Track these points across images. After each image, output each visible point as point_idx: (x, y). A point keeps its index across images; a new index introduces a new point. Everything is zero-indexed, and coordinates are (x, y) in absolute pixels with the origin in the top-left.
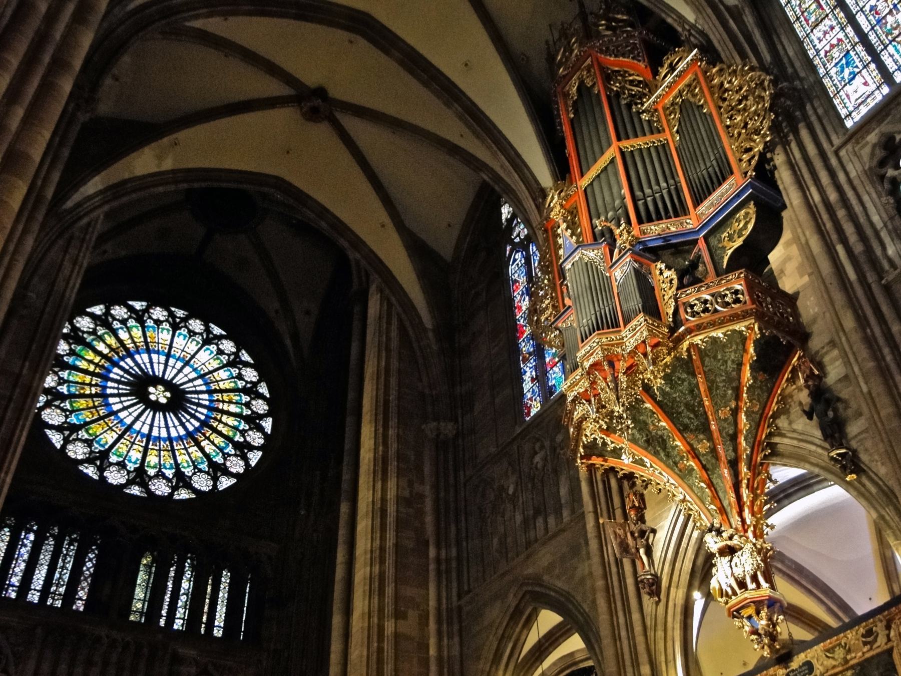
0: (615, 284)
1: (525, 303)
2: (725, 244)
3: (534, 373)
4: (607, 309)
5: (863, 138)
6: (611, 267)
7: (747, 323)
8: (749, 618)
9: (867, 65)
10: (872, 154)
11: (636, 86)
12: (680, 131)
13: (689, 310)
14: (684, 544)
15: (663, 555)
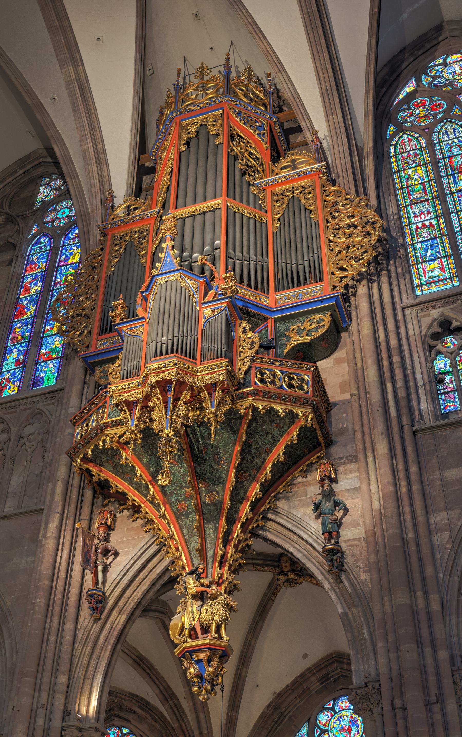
0: (202, 321)
1: (36, 288)
2: (292, 335)
3: (21, 357)
4: (189, 338)
5: (428, 308)
6: (204, 303)
7: (304, 411)
8: (198, 662)
9: (448, 256)
10: (430, 326)
11: (254, 160)
12: (281, 219)
13: (259, 376)
14: (141, 576)
15: (118, 579)
